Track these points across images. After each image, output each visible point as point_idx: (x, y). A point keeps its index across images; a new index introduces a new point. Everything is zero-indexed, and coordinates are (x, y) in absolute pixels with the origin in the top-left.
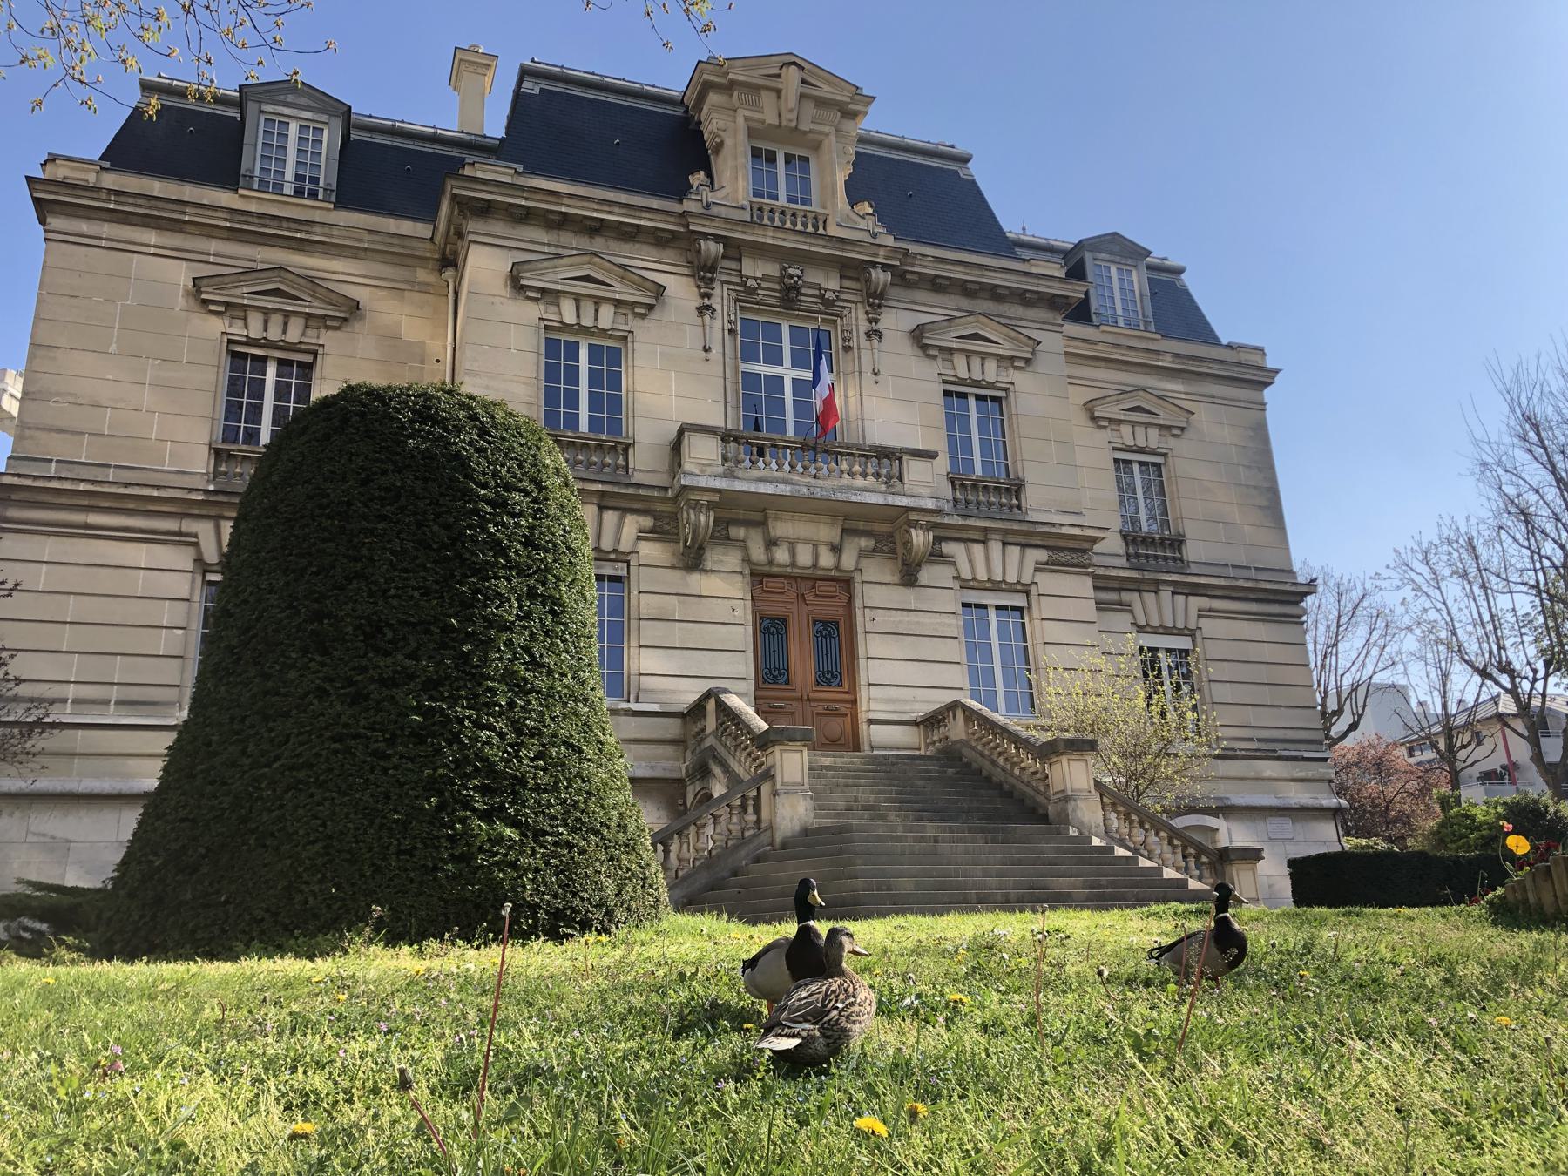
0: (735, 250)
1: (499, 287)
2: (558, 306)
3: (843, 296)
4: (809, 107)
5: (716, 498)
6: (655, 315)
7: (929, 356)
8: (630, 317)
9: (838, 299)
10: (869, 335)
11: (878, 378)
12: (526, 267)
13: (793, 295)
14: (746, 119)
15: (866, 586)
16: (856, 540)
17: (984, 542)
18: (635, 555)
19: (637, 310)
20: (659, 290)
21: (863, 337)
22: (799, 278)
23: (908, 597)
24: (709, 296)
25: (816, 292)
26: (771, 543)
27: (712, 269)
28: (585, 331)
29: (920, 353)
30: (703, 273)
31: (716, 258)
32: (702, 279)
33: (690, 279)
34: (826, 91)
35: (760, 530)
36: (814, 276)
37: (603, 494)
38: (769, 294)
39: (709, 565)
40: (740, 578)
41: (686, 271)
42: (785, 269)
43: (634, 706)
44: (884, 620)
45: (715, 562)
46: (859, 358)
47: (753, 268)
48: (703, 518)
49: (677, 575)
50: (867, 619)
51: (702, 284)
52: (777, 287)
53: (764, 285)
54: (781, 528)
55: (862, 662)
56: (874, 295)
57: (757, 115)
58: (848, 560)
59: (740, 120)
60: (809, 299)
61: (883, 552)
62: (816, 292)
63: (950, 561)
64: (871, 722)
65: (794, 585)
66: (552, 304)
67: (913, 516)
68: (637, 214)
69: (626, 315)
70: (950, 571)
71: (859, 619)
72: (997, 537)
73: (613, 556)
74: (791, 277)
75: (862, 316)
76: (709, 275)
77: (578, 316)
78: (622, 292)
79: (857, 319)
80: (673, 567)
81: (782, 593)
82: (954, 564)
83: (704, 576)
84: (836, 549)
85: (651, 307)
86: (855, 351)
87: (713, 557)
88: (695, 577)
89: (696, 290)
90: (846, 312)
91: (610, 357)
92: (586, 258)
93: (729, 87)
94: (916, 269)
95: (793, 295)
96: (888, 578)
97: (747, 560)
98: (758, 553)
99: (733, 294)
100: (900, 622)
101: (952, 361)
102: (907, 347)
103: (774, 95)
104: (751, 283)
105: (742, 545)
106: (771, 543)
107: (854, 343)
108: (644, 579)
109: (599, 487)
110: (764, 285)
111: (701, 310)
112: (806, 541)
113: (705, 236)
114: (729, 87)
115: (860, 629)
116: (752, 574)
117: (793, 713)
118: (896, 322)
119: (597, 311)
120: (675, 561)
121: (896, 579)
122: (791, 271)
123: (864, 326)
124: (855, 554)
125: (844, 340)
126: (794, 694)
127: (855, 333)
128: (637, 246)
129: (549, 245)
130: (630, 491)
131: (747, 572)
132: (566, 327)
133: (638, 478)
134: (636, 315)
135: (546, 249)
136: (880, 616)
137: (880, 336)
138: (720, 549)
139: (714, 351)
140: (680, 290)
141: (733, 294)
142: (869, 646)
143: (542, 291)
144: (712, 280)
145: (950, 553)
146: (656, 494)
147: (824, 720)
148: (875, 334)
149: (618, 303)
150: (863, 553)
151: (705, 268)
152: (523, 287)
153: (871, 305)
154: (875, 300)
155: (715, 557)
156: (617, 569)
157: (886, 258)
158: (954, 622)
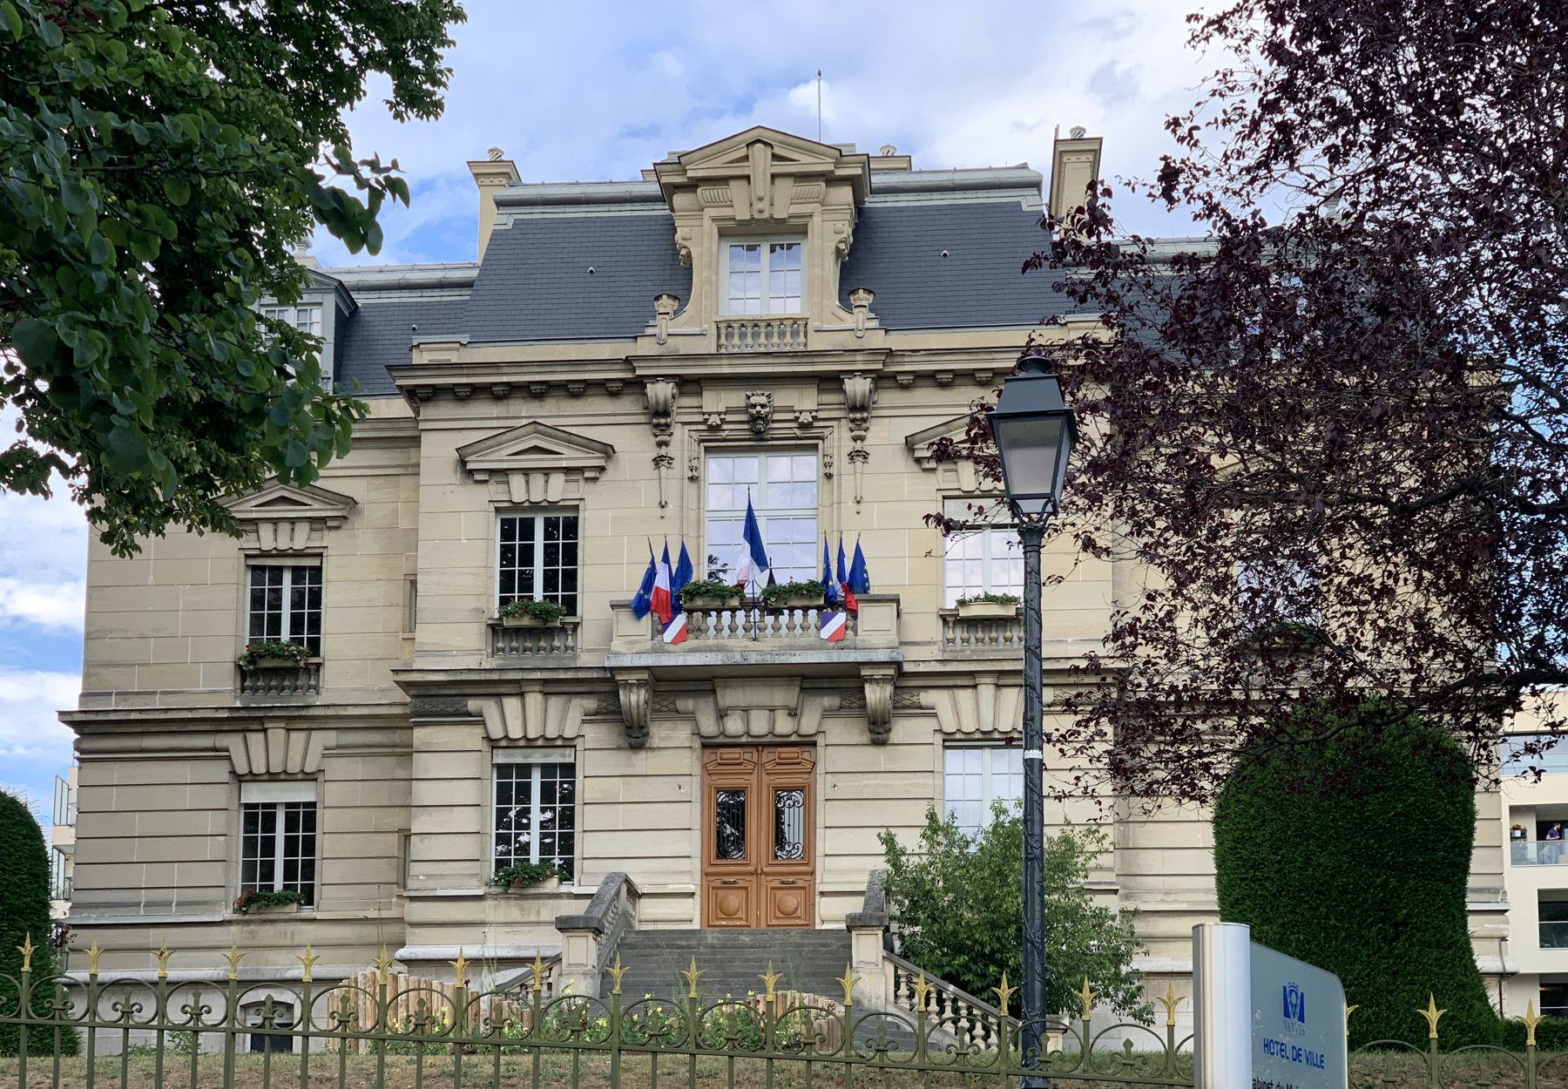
0: (689, 385)
1: (451, 475)
2: (508, 483)
3: (821, 415)
4: (785, 186)
5: (645, 676)
6: (604, 477)
7: (925, 470)
8: (582, 482)
9: (815, 418)
10: (852, 456)
11: (861, 507)
12: (470, 450)
13: (760, 426)
14: (714, 220)
15: (829, 748)
16: (818, 700)
17: (975, 687)
18: (581, 739)
19: (587, 474)
20: (608, 451)
21: (846, 459)
22: (763, 406)
23: (878, 757)
24: (666, 444)
25: (791, 416)
26: (721, 715)
27: (666, 414)
28: (536, 507)
29: (916, 468)
30: (659, 417)
31: (666, 402)
32: (657, 426)
33: (648, 427)
34: (807, 163)
35: (711, 699)
36: (784, 397)
37: (545, 681)
38: (735, 429)
39: (655, 742)
40: (687, 753)
41: (642, 419)
42: (748, 397)
43: (576, 890)
44: (846, 786)
45: (663, 739)
46: (839, 486)
47: (715, 402)
48: (634, 698)
49: (623, 755)
50: (828, 785)
51: (658, 432)
52: (744, 418)
53: (729, 418)
54: (730, 697)
55: (820, 832)
56: (853, 408)
57: (727, 212)
58: (809, 724)
59: (707, 222)
60: (781, 428)
61: (850, 708)
62: (791, 416)
63: (930, 712)
64: (822, 894)
65: (755, 754)
66: (501, 482)
67: (865, 672)
68: (580, 368)
69: (577, 481)
70: (931, 724)
71: (820, 786)
72: (988, 680)
73: (559, 743)
74: (754, 406)
75: (847, 435)
76: (662, 421)
77: (528, 492)
78: (571, 457)
79: (839, 439)
80: (619, 748)
81: (741, 764)
82: (935, 715)
83: (650, 754)
84: (793, 713)
85: (602, 469)
86: (835, 478)
87: (660, 733)
88: (642, 754)
89: (653, 438)
90: (827, 432)
91: (565, 527)
92: (531, 428)
93: (693, 185)
94: (906, 368)
95: (760, 426)
96: (856, 739)
97: (697, 733)
98: (709, 726)
99: (695, 435)
100: (866, 786)
101: (956, 471)
102: (902, 463)
103: (745, 183)
104: (714, 420)
105: (690, 717)
106: (721, 715)
107: (834, 471)
108: (587, 764)
109: (538, 675)
110: (729, 418)
111: (658, 461)
112: (759, 708)
113: (654, 378)
114: (693, 185)
115: (820, 797)
116: (704, 746)
117: (746, 888)
118: (886, 433)
119: (547, 481)
120: (622, 742)
121: (866, 738)
122: (753, 400)
123: (849, 446)
124: (817, 716)
125: (825, 465)
126: (751, 869)
127: (835, 457)
128: (590, 400)
129: (498, 418)
130: (569, 675)
131: (697, 745)
132: (516, 506)
133: (585, 660)
134: (587, 479)
135: (495, 424)
136: (841, 781)
137: (865, 456)
138: (668, 724)
139: (670, 506)
140: (632, 443)
141: (695, 435)
142: (826, 814)
143: (491, 472)
144: (668, 426)
145: (930, 704)
146: (595, 675)
147: (779, 894)
148: (858, 455)
149: (568, 471)
150: (827, 713)
151: (657, 414)
152: (471, 473)
153: (853, 421)
154: (859, 412)
155: (663, 734)
156: (563, 756)
157: (866, 362)
158: (930, 781)
